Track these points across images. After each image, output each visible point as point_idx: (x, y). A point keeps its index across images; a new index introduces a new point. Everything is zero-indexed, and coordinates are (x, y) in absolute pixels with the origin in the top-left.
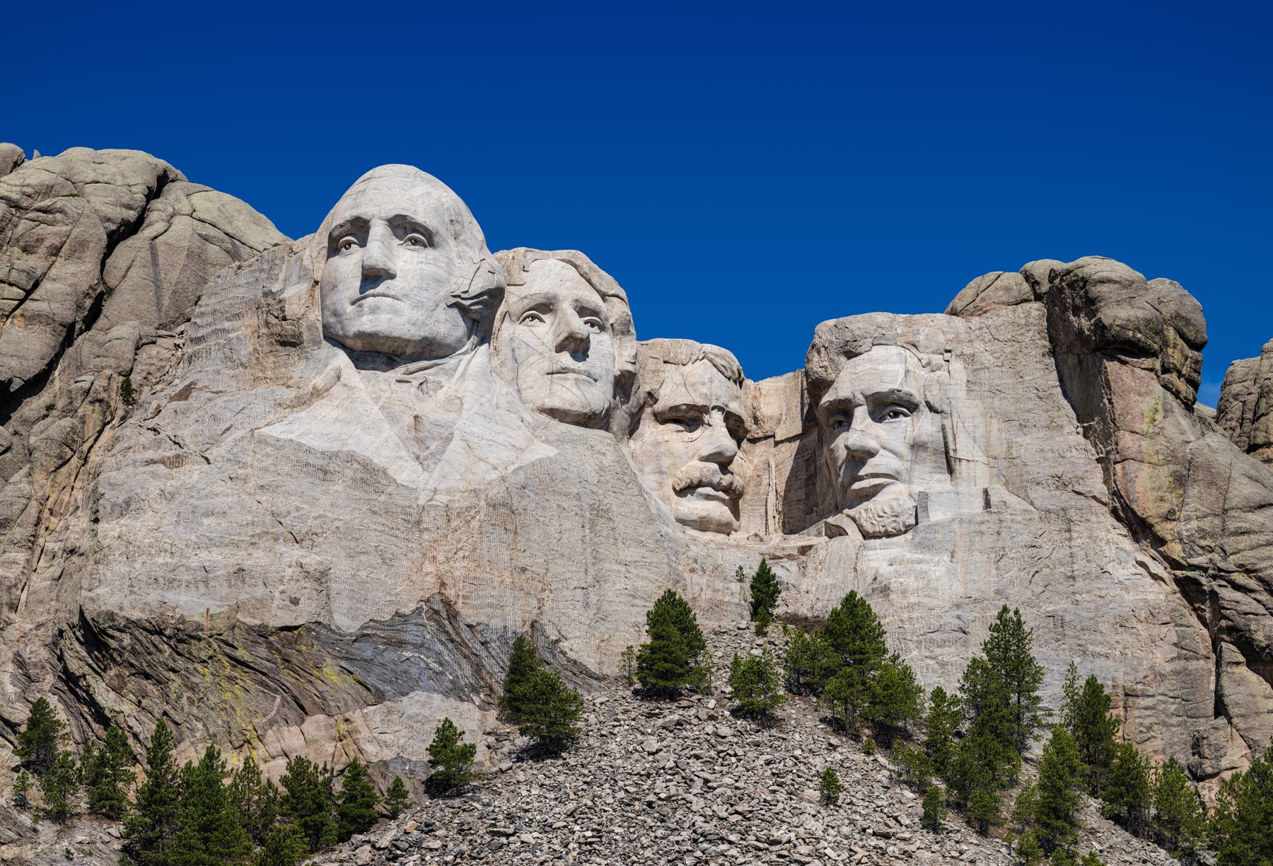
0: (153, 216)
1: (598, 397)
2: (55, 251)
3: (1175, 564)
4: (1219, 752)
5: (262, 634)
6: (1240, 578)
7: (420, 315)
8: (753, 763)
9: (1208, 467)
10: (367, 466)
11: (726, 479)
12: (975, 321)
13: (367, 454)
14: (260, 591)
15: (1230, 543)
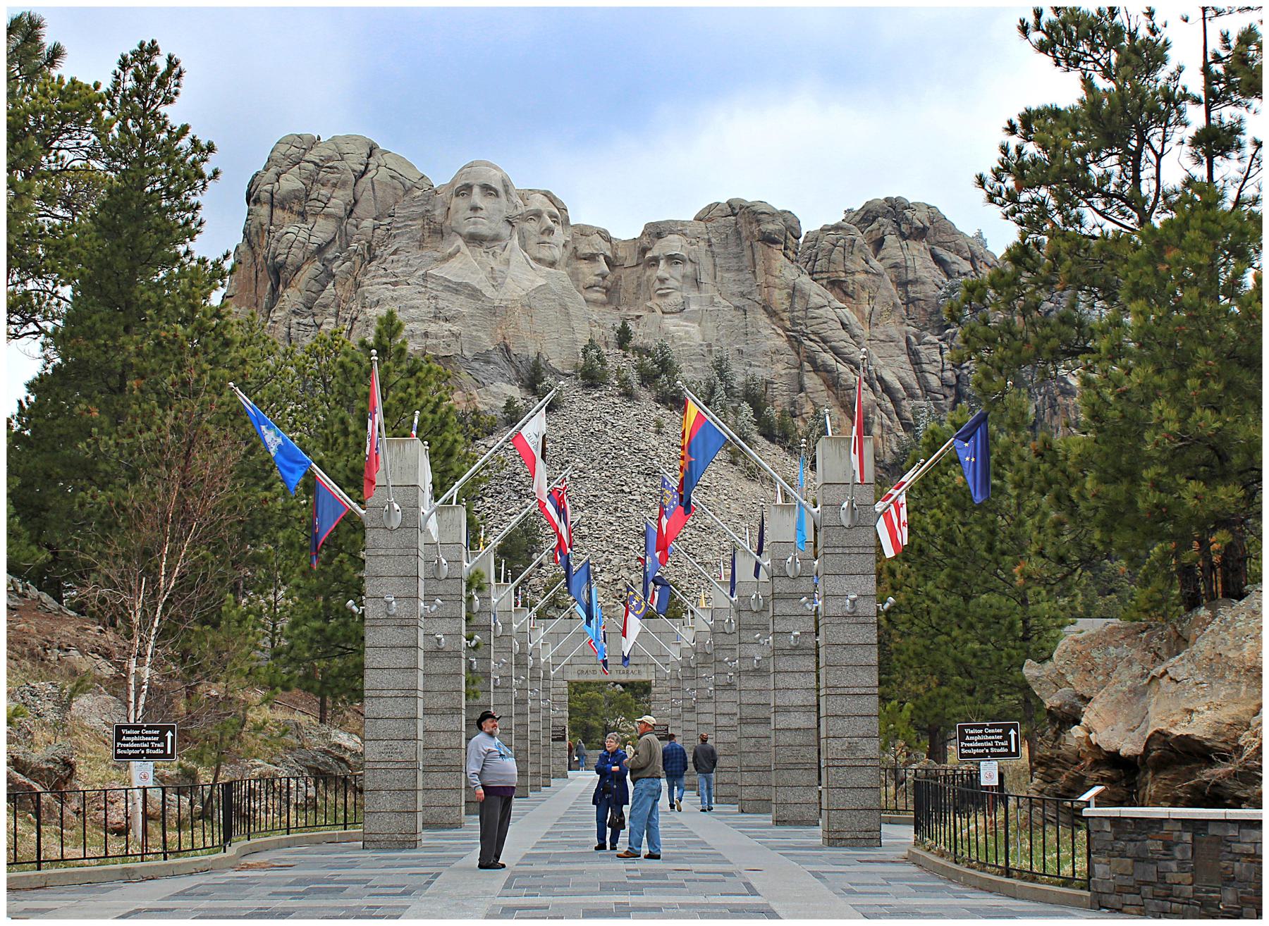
0: (370, 167)
1: (557, 253)
2: (335, 185)
3: (786, 330)
4: (802, 407)
5: (437, 358)
6: (812, 337)
7: (493, 225)
8: (630, 415)
9: (801, 291)
10: (475, 289)
11: (607, 283)
12: (709, 224)
13: (474, 284)
14: (434, 341)
15: (809, 322)
